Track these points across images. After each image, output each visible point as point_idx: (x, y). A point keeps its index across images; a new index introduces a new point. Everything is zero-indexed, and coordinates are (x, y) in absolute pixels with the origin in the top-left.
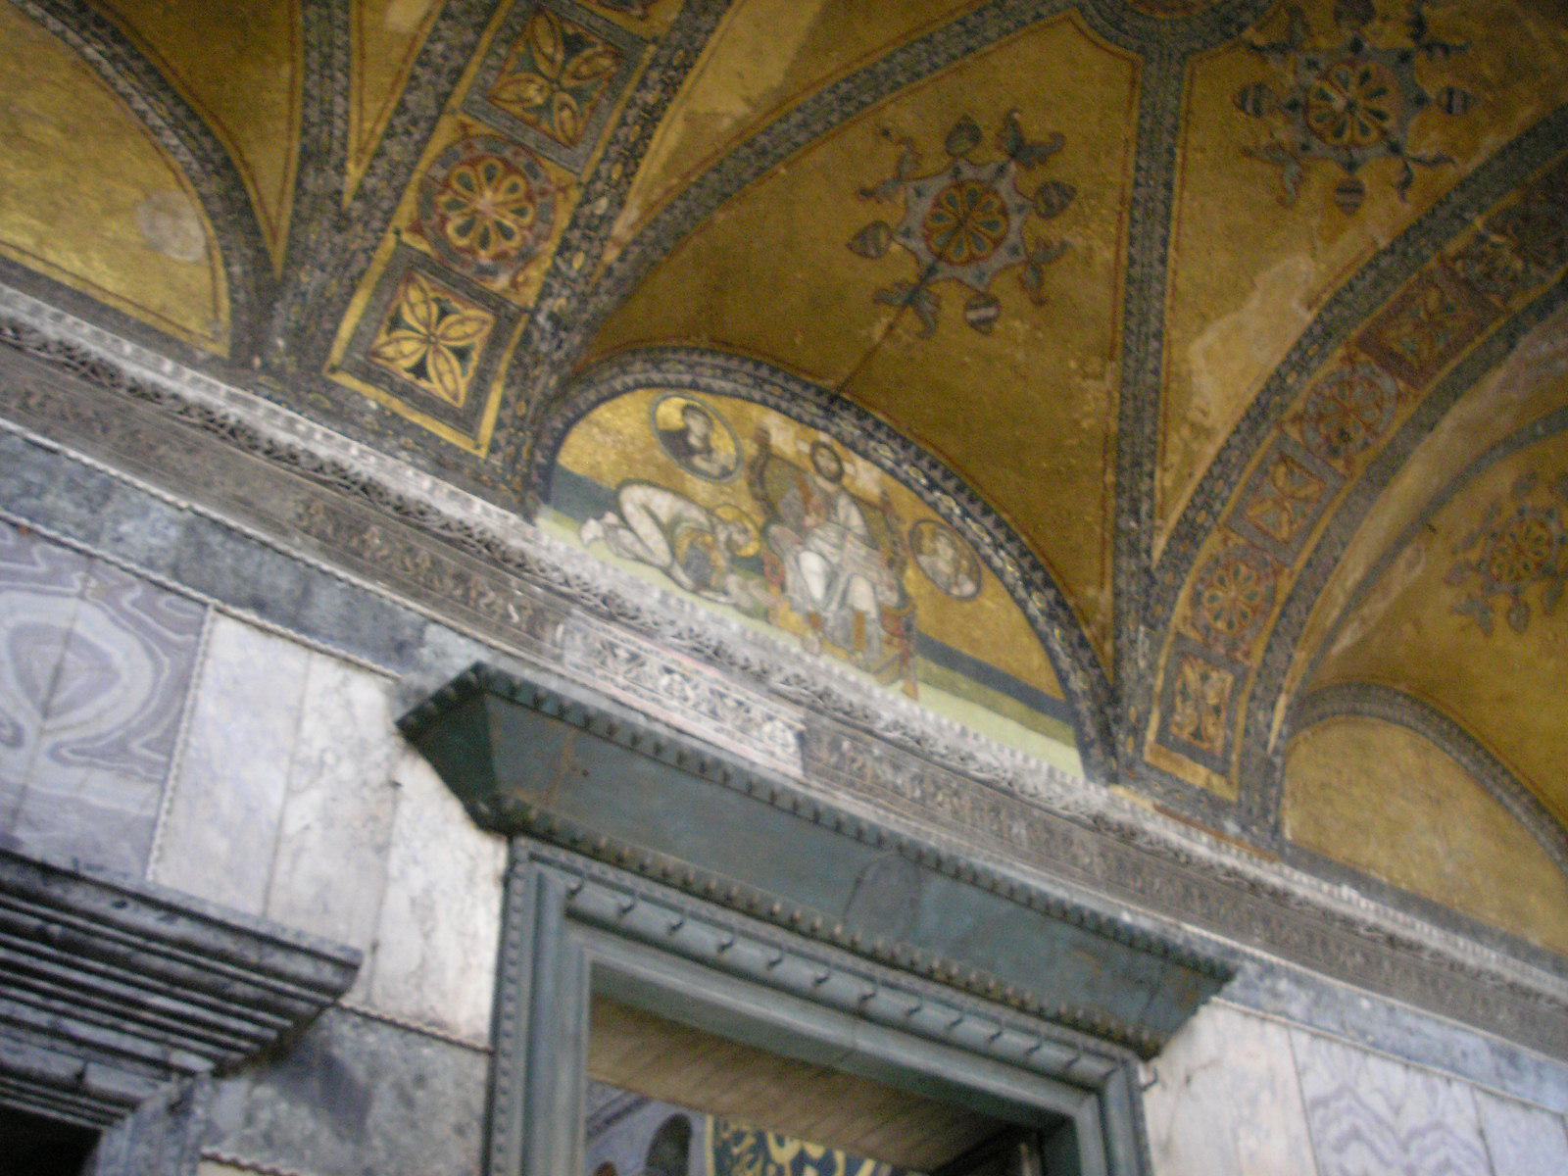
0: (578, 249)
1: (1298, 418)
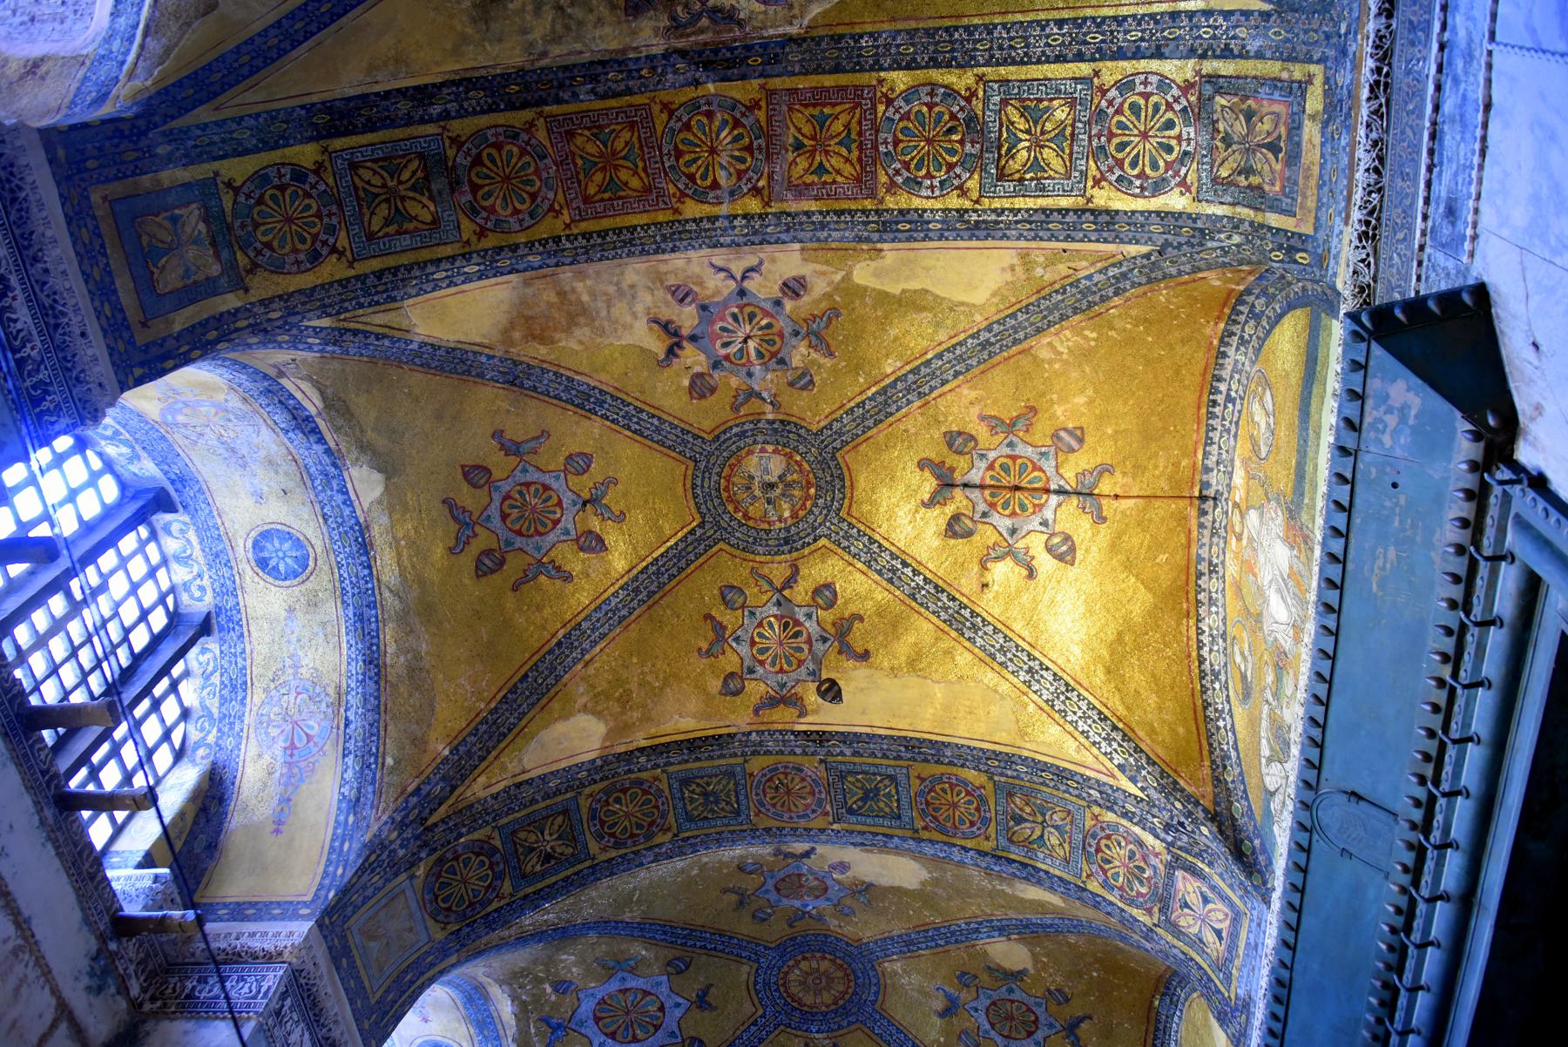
1: (963, 192)
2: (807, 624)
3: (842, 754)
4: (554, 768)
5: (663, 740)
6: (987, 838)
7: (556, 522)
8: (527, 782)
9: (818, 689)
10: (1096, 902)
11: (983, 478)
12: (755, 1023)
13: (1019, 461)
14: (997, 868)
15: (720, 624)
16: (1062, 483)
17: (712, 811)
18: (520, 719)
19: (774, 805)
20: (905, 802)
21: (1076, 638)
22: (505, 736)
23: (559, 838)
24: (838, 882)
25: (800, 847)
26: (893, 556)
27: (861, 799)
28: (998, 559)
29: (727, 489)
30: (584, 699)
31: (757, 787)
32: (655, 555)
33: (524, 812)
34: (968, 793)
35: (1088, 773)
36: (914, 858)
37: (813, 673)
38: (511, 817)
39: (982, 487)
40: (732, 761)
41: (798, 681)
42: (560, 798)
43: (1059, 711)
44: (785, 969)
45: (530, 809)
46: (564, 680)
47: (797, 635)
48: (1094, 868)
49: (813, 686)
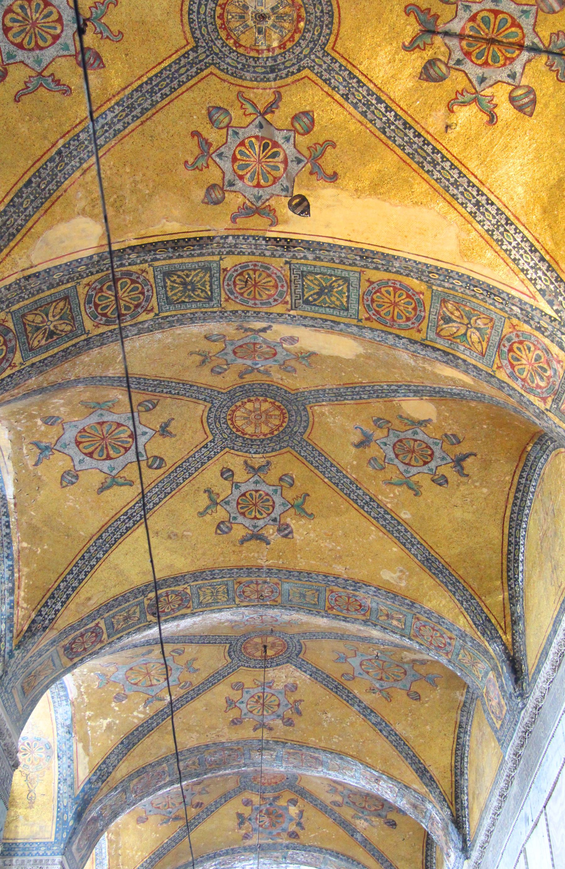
0: (539, 323)
2: (285, 146)
3: (305, 258)
4: (57, 263)
5: (151, 240)
6: (419, 331)
7: (56, 38)
8: (34, 275)
9: (290, 204)
10: (501, 386)
11: (463, 28)
12: (206, 446)
13: (501, 16)
14: (424, 353)
15: (206, 141)
16: (536, 40)
17: (190, 297)
18: (27, 221)
19: (242, 294)
20: (353, 297)
21: (523, 179)
22: (14, 235)
23: (61, 318)
24: (287, 350)
25: (259, 325)
26: (370, 93)
27: (317, 293)
28: (464, 104)
29: (221, 17)
30: (82, 204)
31: (229, 279)
32: (150, 75)
33: (32, 300)
34: (408, 296)
35: (513, 293)
36: (355, 339)
37: (286, 189)
38: (21, 304)
39: (461, 37)
40: (210, 258)
41: (272, 196)
42: (64, 287)
43: (497, 241)
44: (233, 408)
45: (37, 298)
46: (64, 186)
47: (275, 155)
48: (505, 362)
49: (286, 201)
